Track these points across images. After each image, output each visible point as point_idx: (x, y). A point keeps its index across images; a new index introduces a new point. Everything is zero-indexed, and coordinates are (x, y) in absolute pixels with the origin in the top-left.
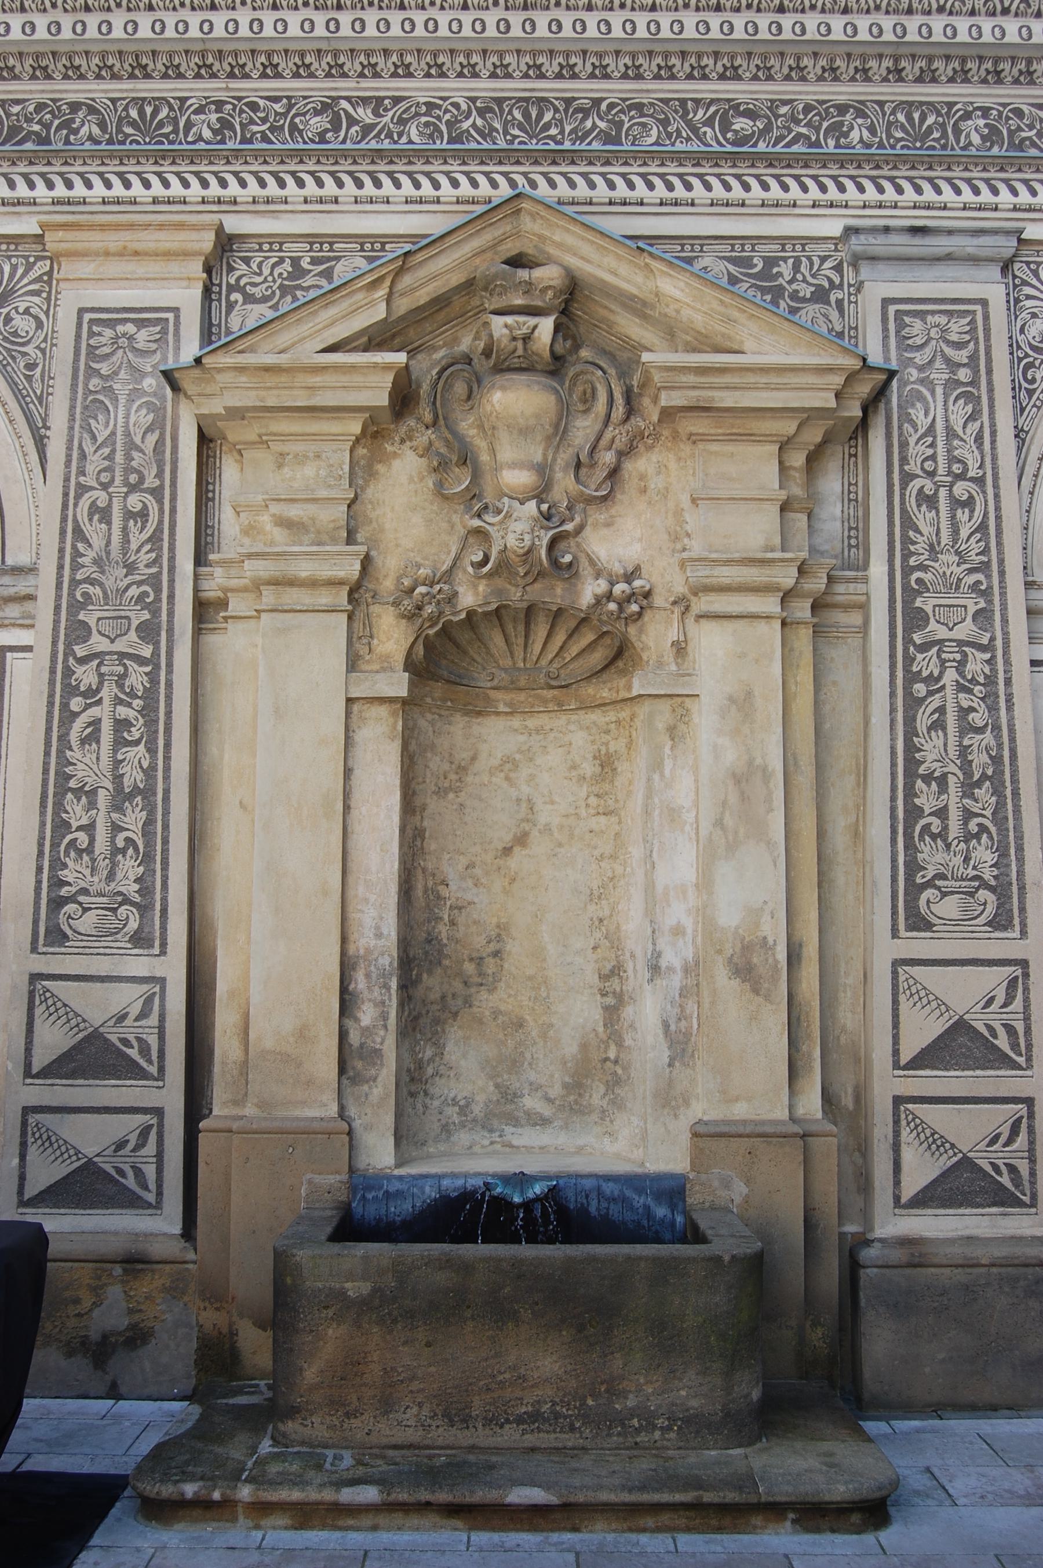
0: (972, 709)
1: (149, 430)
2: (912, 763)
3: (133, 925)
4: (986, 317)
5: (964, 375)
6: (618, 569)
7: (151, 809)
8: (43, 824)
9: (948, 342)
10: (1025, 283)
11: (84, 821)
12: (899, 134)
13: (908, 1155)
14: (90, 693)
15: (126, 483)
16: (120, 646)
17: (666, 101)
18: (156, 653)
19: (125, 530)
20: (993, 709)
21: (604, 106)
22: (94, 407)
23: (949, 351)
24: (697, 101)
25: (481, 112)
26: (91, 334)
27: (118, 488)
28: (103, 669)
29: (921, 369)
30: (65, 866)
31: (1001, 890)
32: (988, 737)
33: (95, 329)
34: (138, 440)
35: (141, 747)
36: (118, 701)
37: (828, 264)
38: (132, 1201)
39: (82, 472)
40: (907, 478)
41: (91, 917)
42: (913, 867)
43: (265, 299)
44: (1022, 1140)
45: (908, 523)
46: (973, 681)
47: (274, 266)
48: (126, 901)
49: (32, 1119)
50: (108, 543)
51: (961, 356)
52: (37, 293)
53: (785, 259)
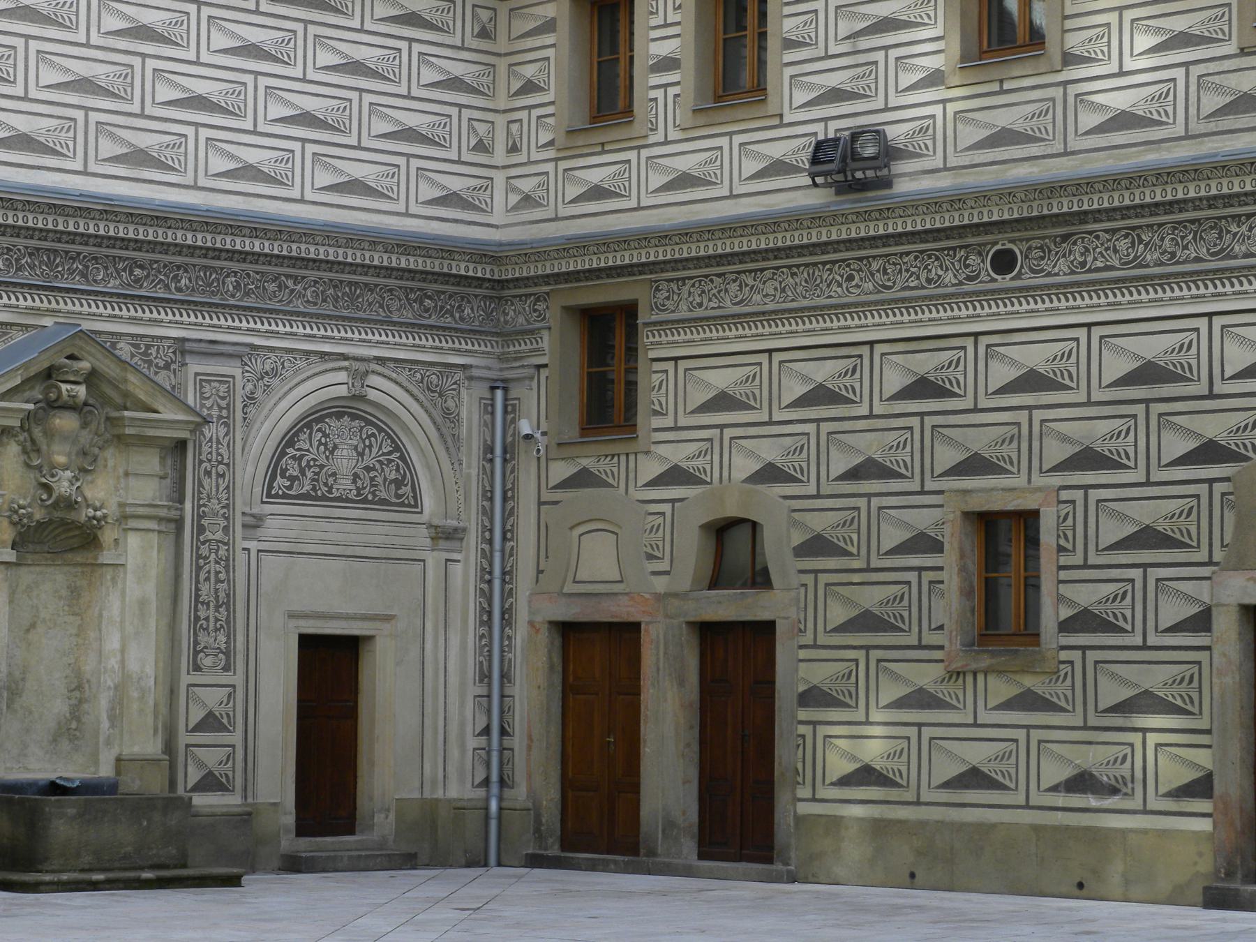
0: (220, 572)
2: (197, 596)
4: (234, 385)
5: (224, 413)
9: (220, 397)
10: (246, 364)
12: (201, 283)
13: (190, 769)
17: (107, 256)
20: (228, 572)
24: (120, 258)
25: (30, 255)
29: (208, 409)
37: (171, 350)
40: (201, 462)
42: (196, 643)
45: (201, 485)
46: (221, 559)
51: (223, 403)
53: (153, 346)
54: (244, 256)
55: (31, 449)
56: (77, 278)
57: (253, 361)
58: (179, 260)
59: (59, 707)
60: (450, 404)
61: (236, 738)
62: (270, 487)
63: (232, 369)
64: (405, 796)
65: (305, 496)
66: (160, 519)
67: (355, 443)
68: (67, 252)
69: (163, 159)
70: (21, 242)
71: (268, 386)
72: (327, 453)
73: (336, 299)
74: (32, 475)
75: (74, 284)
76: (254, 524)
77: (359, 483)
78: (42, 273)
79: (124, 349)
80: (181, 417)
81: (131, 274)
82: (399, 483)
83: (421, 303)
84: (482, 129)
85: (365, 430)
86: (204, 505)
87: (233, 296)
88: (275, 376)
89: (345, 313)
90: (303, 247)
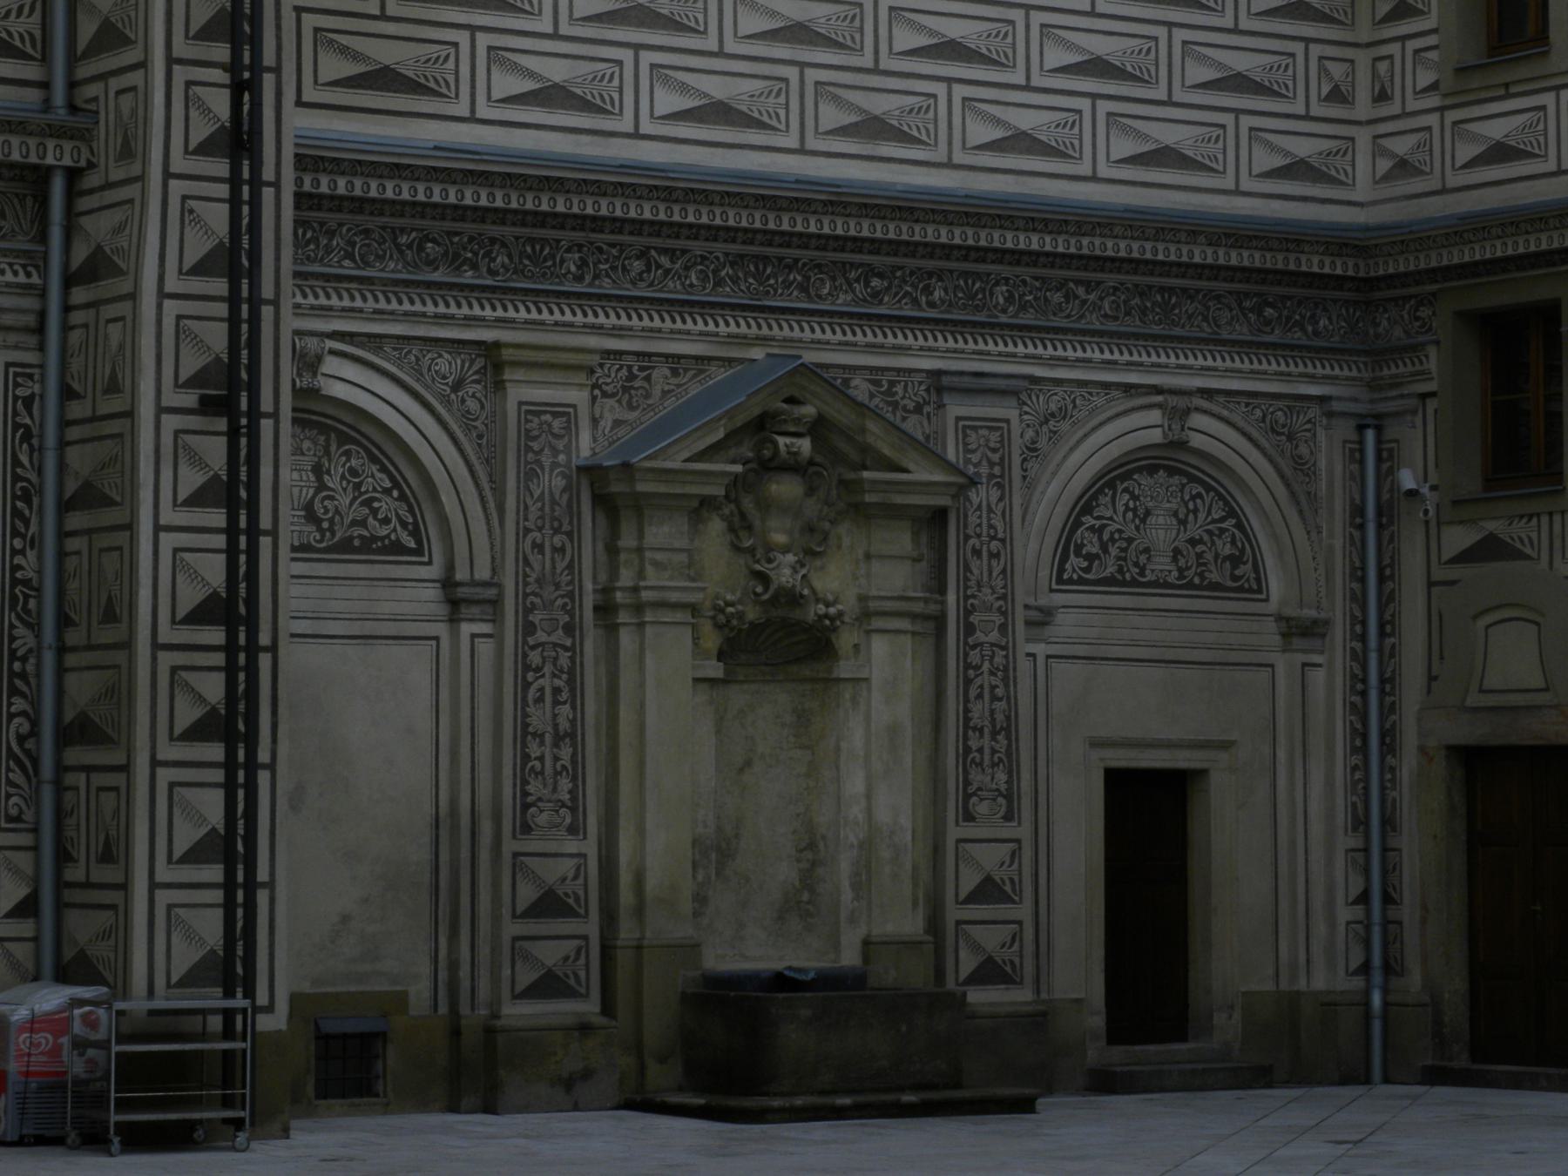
0: (997, 686)
1: (564, 491)
2: (967, 719)
3: (568, 820)
7: (574, 745)
8: (515, 755)
9: (990, 449)
11: (538, 754)
12: (960, 295)
13: (963, 954)
14: (538, 669)
15: (552, 528)
16: (553, 639)
17: (834, 263)
18: (574, 644)
19: (553, 560)
20: (1007, 686)
21: (800, 265)
23: (990, 454)
24: (852, 265)
25: (732, 264)
26: (527, 421)
27: (548, 531)
28: (545, 654)
29: (975, 465)
30: (528, 783)
31: (1008, 797)
32: (1004, 703)
33: (529, 417)
34: (557, 497)
35: (568, 706)
36: (554, 675)
37: (923, 387)
38: (571, 993)
39: (526, 519)
40: (967, 537)
41: (545, 816)
42: (967, 783)
43: (613, 395)
44: (1016, 946)
45: (967, 568)
46: (998, 669)
47: (618, 370)
48: (564, 805)
49: (518, 944)
50: (544, 568)
51: (996, 457)
52: (477, 382)
53: (899, 382)
55: (740, 525)
56: (795, 293)
57: (1034, 398)
59: (785, 872)
60: (1304, 450)
61: (1024, 911)
62: (1061, 570)
63: (1006, 410)
65: (1109, 581)
66: (914, 616)
67: (1174, 506)
68: (781, 259)
69: (906, 128)
70: (719, 248)
71: (1055, 433)
72: (1137, 521)
73: (1144, 311)
75: (791, 301)
76: (1041, 620)
77: (1182, 563)
78: (748, 288)
79: (860, 388)
81: (867, 285)
82: (1236, 560)
83: (1260, 314)
84: (1337, 70)
85: (1187, 489)
86: (974, 596)
87: (1004, 311)
88: (1064, 418)
89: (1156, 329)
90: (1097, 241)
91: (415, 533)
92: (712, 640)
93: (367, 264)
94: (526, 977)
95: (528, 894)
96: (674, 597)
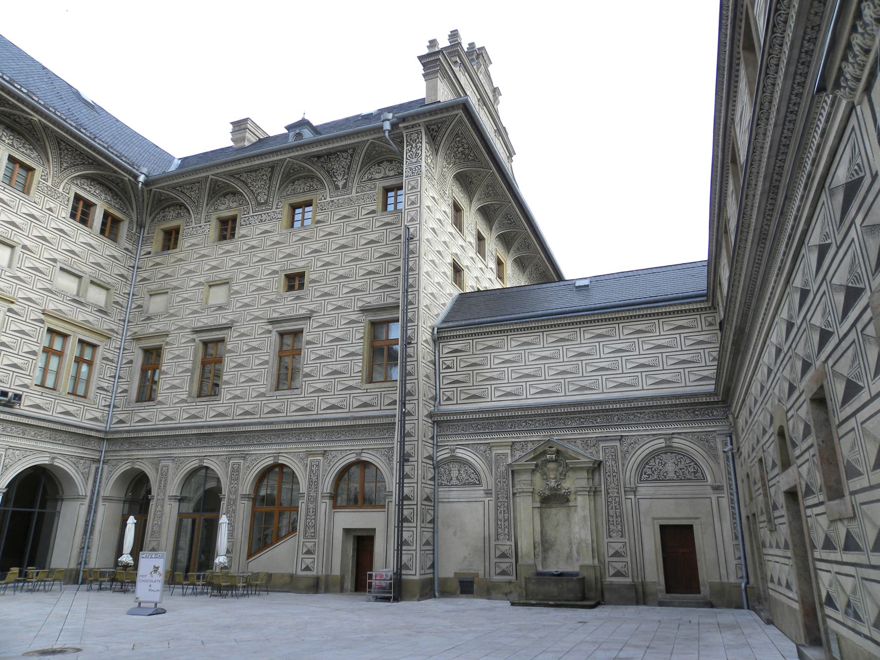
5: (614, 457)
6: (566, 488)
13: (610, 569)
20: (620, 506)
22: (498, 467)
31: (622, 532)
38: (509, 575)
40: (606, 473)
42: (609, 529)
45: (607, 479)
51: (614, 454)
54: (617, 410)
55: (544, 474)
58: (596, 414)
60: (712, 444)
61: (628, 559)
62: (641, 478)
64: (714, 581)
65: (656, 480)
67: (673, 461)
74: (545, 482)
77: (678, 474)
80: (587, 460)
82: (695, 473)
83: (694, 413)
87: (617, 422)
91: (479, 481)
92: (538, 499)
93: (466, 431)
94: (498, 571)
95: (498, 553)
96: (525, 490)
